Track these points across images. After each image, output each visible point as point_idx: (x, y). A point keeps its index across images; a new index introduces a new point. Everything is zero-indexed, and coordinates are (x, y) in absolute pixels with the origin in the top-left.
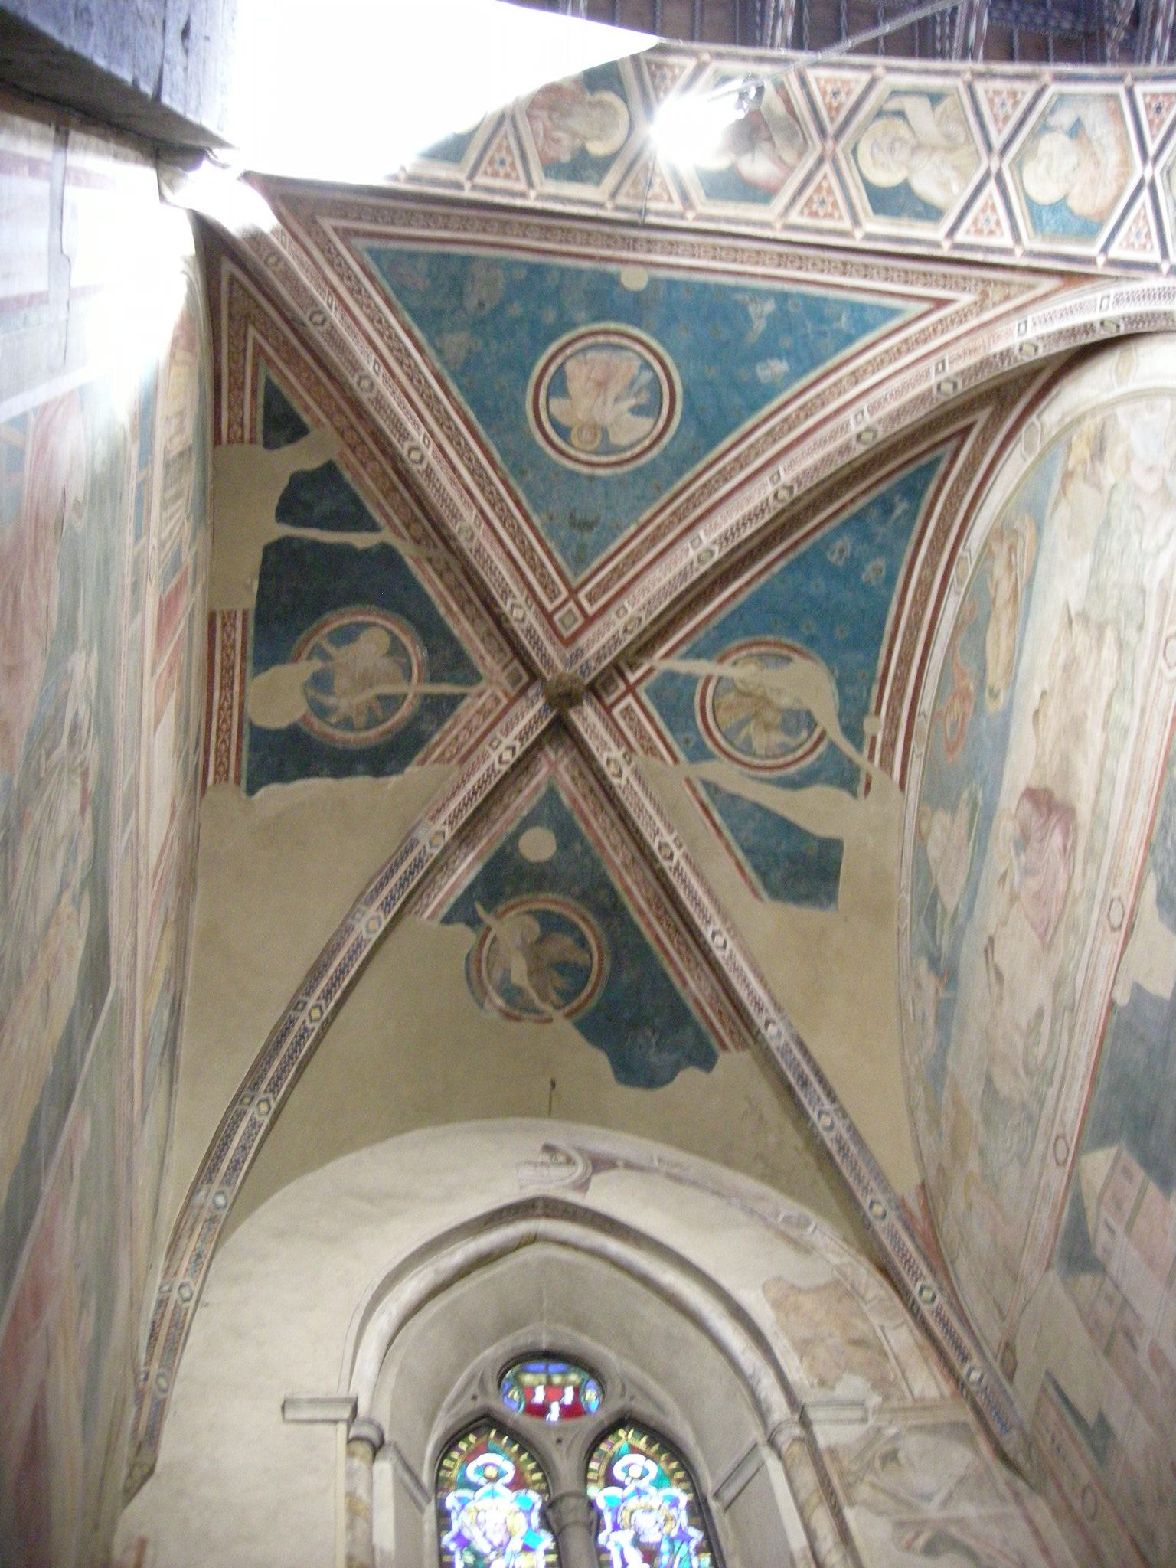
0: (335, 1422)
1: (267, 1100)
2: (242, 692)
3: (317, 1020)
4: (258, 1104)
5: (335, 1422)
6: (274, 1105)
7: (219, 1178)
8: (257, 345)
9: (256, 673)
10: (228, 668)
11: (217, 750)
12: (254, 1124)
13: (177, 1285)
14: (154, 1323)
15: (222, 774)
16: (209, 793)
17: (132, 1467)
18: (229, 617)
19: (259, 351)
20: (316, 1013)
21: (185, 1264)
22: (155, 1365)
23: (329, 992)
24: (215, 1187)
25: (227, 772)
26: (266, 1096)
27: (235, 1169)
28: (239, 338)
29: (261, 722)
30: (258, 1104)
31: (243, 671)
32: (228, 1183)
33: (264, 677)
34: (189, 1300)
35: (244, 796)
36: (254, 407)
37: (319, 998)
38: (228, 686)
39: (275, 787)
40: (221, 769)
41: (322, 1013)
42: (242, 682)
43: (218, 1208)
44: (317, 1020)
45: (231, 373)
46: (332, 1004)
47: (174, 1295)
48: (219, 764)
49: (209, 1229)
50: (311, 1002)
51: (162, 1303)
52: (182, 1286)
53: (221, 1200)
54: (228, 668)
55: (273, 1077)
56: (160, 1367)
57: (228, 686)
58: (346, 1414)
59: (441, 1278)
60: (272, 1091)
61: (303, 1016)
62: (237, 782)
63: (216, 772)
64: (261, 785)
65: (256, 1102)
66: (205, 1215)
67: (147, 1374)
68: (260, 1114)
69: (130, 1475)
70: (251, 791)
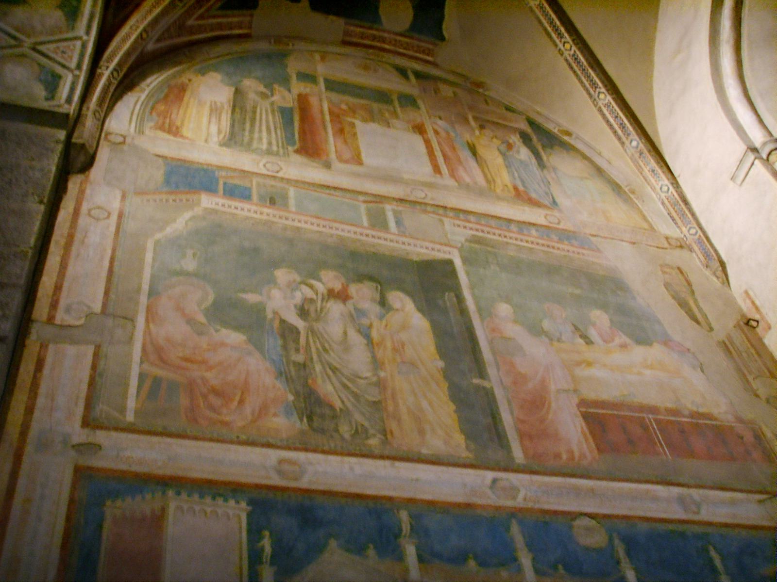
0: (753, 164)
1: (599, 93)
2: (389, 32)
3: (571, 47)
4: (599, 99)
5: (753, 164)
6: (603, 90)
7: (624, 138)
8: (197, 19)
9: (380, 23)
10: (374, 38)
11: (416, 52)
12: (608, 105)
13: (659, 191)
14: (669, 214)
15: (429, 52)
16: (439, 61)
17: (714, 274)
18: (346, 33)
19: (201, 17)
20: (567, 46)
21: (653, 181)
22: (684, 229)
23: (559, 34)
24: (627, 143)
25: (429, 50)
26: (597, 93)
27: (624, 127)
28: (192, 31)
29: (407, 25)
30: (599, 99)
31: (377, 30)
32: (629, 135)
33: (384, 19)
34: (668, 189)
35: (444, 43)
36: (234, 16)
37: (561, 41)
38: (383, 40)
39: (444, 26)
40: (427, 52)
41: (568, 42)
42: (384, 31)
43: (637, 147)
44: (571, 47)
45: (212, 30)
46: (566, 35)
47: (663, 195)
48: (423, 52)
49: (644, 157)
50: (561, 46)
51: (663, 203)
52: (661, 189)
53: (634, 143)
54: (374, 38)
55: (590, 84)
56: (686, 227)
57: (383, 40)
58: (751, 156)
59: (732, 42)
60: (596, 88)
61: (566, 54)
62: (435, 45)
63: (428, 55)
64: (441, 33)
65: (597, 99)
66: (637, 155)
67: (685, 236)
68: (604, 100)
69: (718, 278)
70: (443, 39)
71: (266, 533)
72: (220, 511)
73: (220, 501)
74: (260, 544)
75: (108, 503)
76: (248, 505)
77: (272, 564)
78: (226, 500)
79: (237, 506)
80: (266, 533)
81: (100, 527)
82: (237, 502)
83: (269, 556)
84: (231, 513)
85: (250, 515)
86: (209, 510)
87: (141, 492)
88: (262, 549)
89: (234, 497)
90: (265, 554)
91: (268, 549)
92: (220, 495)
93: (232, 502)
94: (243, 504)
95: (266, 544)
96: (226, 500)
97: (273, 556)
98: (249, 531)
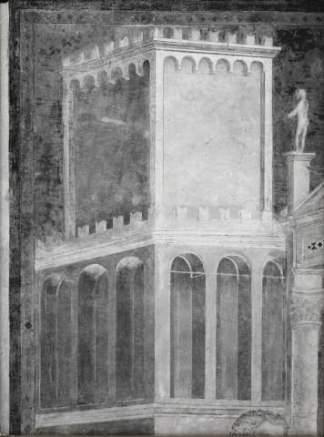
71: (302, 93)
72: (231, 60)
73: (232, 40)
74: (291, 115)
75: (66, 63)
76: (275, 44)
77: (307, 149)
78: (241, 39)
79: (258, 47)
80: (302, 93)
81: (58, 107)
82: (259, 41)
83: (304, 135)
84: (248, 60)
85: (277, 61)
86: (214, 59)
87: (113, 38)
88: (295, 121)
89: (253, 32)
90: (299, 132)
91: (303, 123)
92: (234, 29)
93: (250, 41)
94: (268, 44)
95: (301, 113)
96: (241, 39)
97: (310, 135)
98: (277, 91)
